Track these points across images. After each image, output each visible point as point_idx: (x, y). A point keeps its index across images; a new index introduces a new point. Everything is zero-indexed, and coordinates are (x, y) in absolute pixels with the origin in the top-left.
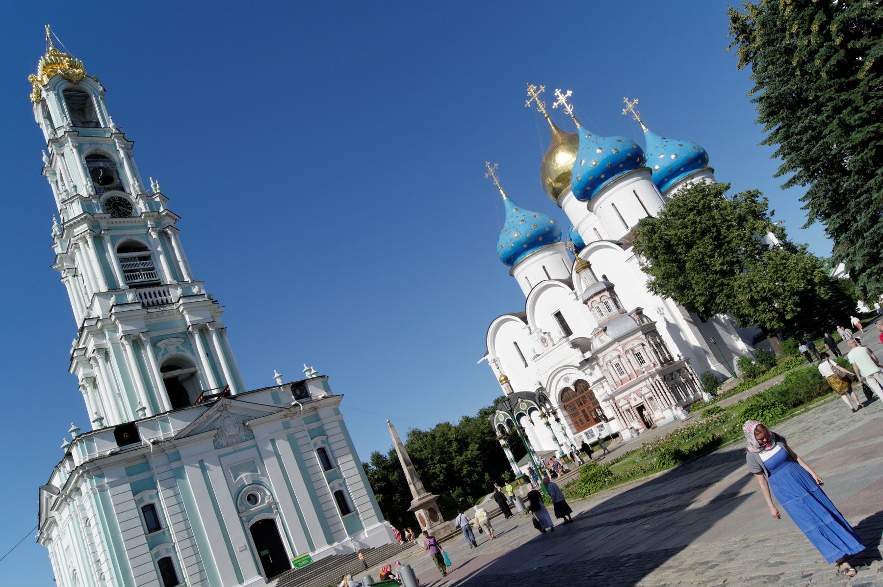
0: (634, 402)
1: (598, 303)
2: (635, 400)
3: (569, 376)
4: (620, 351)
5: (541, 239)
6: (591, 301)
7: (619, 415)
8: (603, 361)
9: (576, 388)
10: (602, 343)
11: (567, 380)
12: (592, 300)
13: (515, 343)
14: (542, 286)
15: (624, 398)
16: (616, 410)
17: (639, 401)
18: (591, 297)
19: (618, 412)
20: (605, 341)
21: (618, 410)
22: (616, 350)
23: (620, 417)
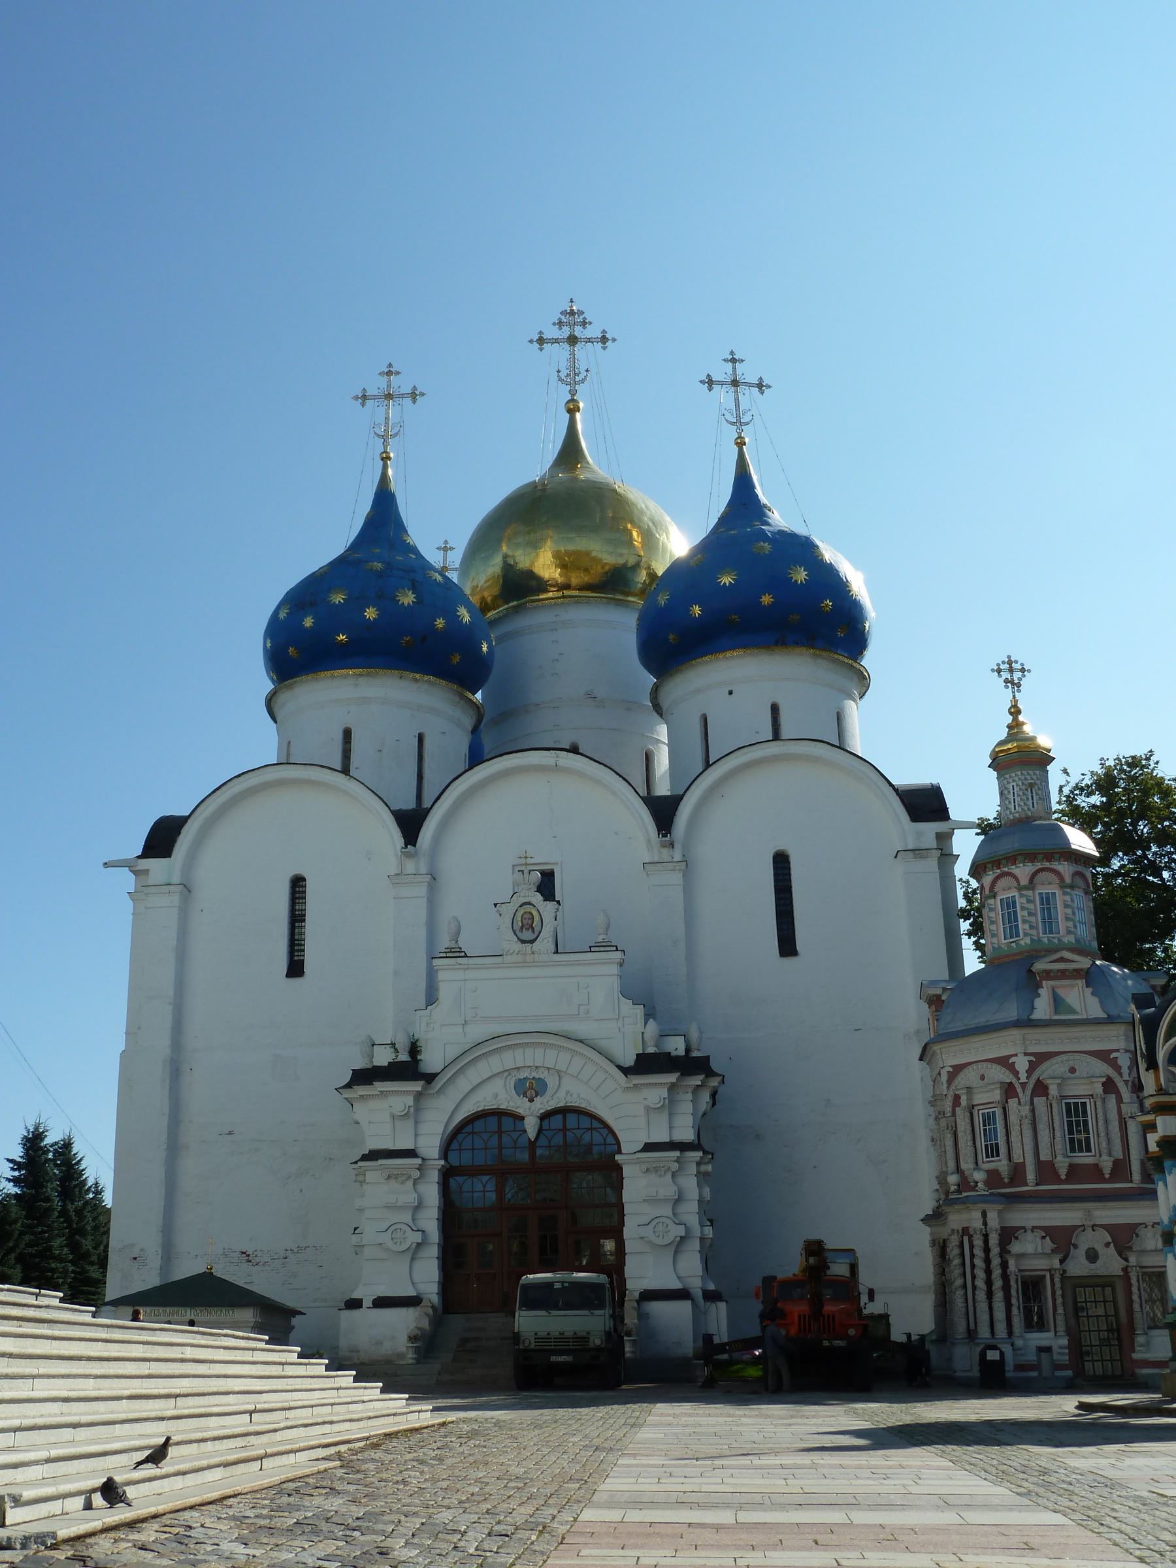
0: (1086, 1262)
1: (1020, 888)
2: (1092, 1256)
3: (551, 1082)
4: (1118, 1069)
5: (456, 659)
6: (1039, 865)
7: (998, 1284)
8: (1030, 1072)
9: (540, 1131)
10: (1056, 1012)
11: (531, 1088)
12: (1047, 865)
13: (298, 884)
14: (552, 762)
15: (1049, 1232)
16: (996, 1262)
17: (1110, 1263)
18: (1049, 856)
19: (997, 1273)
20: (1074, 1012)
21: (1004, 1265)
22: (1103, 1056)
23: (999, 1296)
